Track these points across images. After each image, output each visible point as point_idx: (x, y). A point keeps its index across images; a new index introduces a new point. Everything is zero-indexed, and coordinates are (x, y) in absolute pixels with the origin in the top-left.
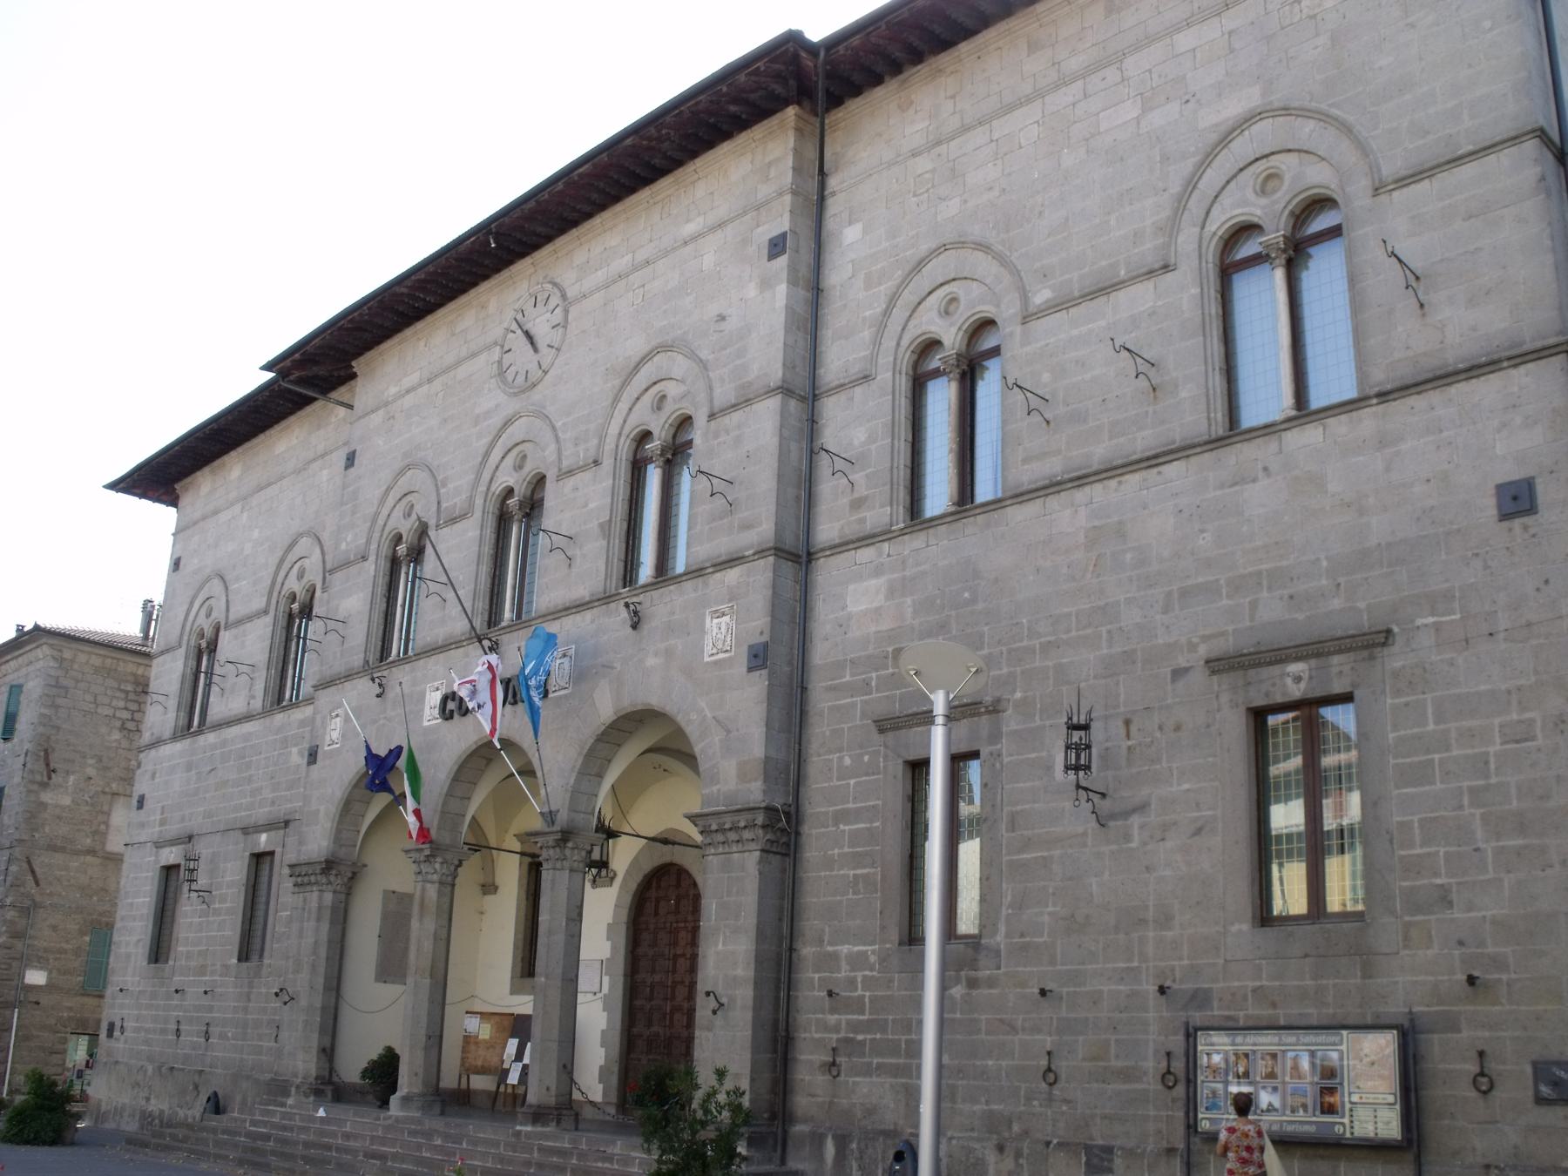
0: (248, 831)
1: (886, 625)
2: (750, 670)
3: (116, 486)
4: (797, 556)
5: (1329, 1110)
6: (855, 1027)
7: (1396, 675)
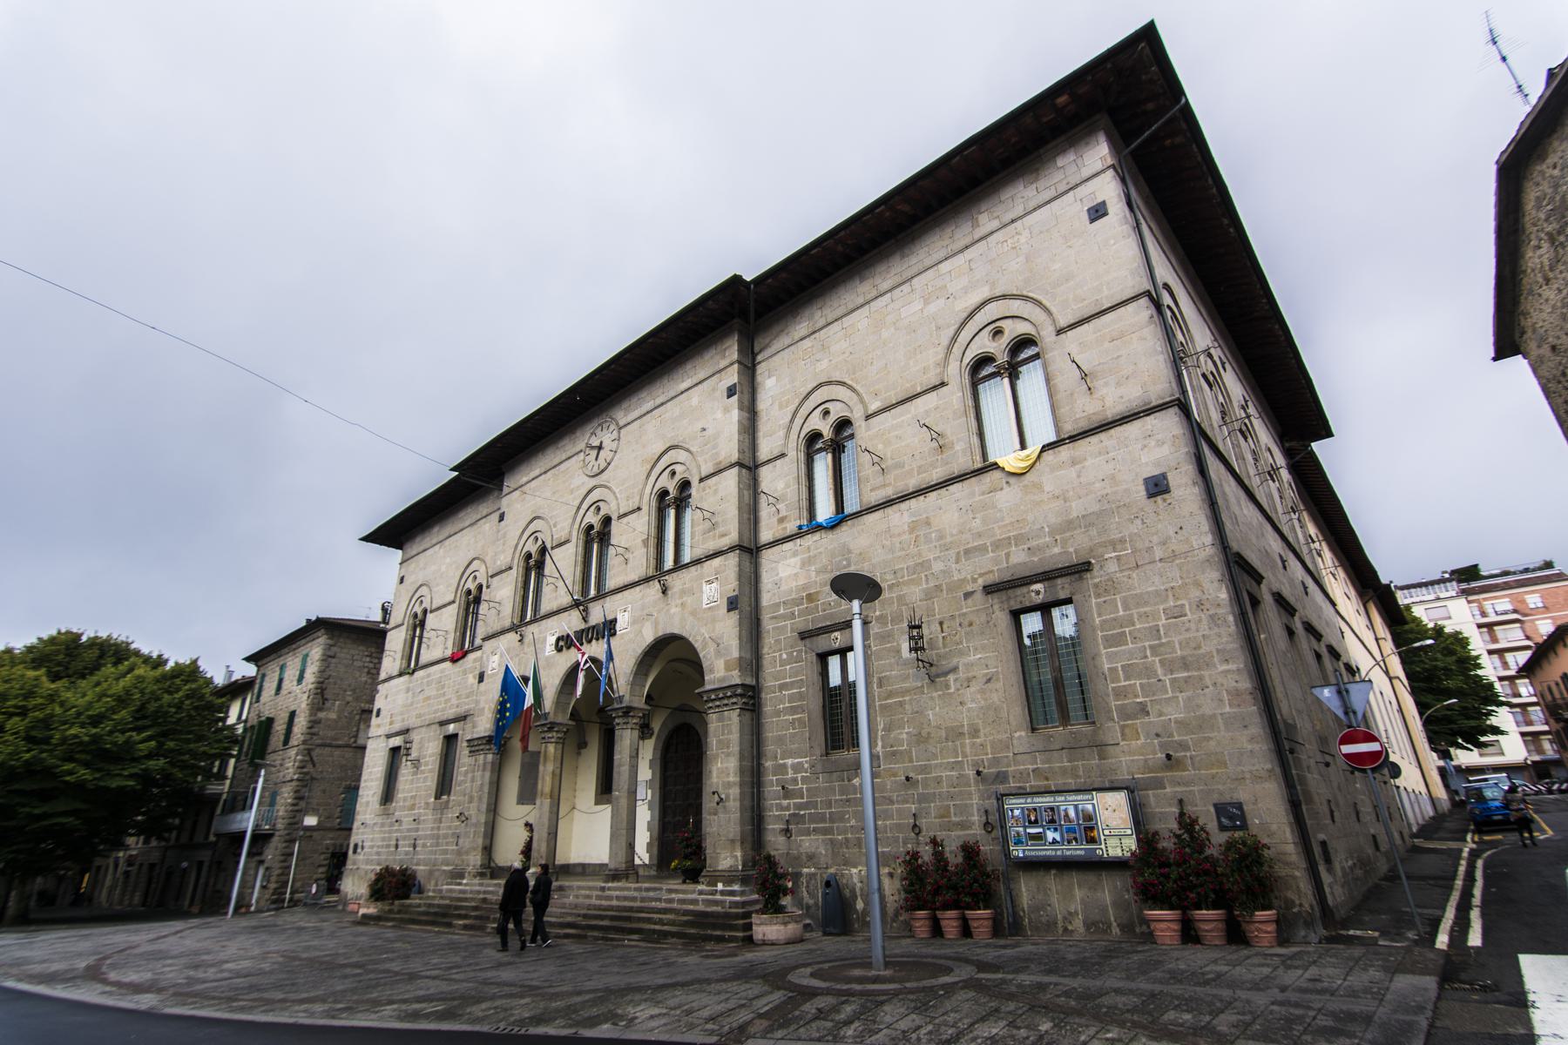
0: (443, 723)
3: (367, 539)
4: (750, 550)
5: (1092, 840)
6: (799, 807)
7: (1096, 586)
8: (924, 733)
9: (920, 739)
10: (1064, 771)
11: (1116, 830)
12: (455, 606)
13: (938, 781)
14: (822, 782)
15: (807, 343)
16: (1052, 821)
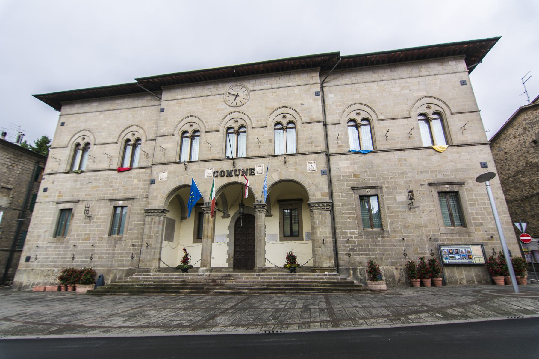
1: (350, 170)
2: (322, 175)
5: (471, 258)
6: (354, 246)
7: (466, 189)
8: (407, 225)
9: (405, 227)
10: (457, 239)
11: (478, 257)
12: (119, 145)
13: (413, 240)
14: (364, 238)
15: (349, 87)
16: (457, 253)
